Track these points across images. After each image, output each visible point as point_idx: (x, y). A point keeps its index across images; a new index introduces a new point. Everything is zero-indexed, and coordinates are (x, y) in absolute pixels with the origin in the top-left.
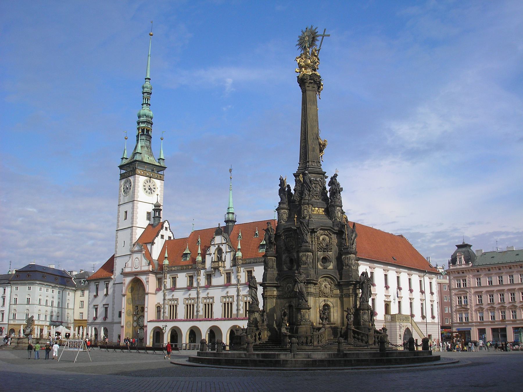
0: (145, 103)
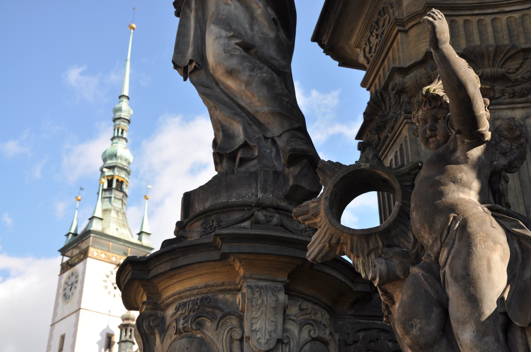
0: (118, 137)
